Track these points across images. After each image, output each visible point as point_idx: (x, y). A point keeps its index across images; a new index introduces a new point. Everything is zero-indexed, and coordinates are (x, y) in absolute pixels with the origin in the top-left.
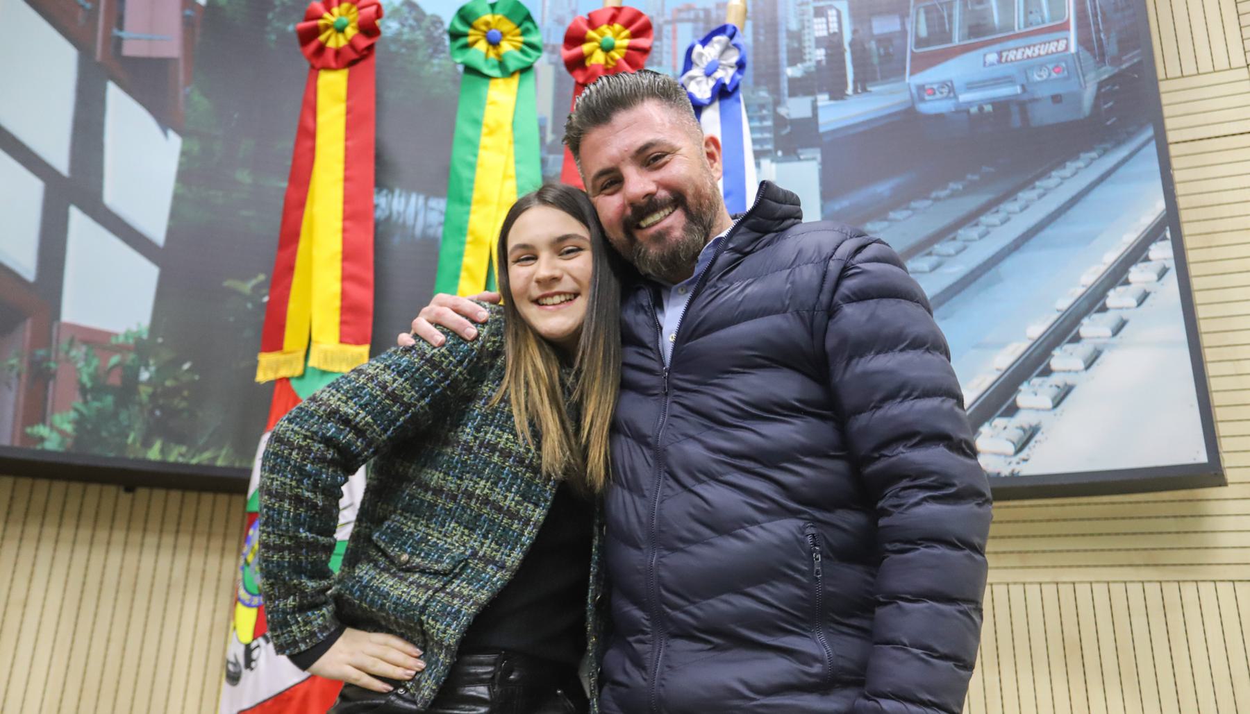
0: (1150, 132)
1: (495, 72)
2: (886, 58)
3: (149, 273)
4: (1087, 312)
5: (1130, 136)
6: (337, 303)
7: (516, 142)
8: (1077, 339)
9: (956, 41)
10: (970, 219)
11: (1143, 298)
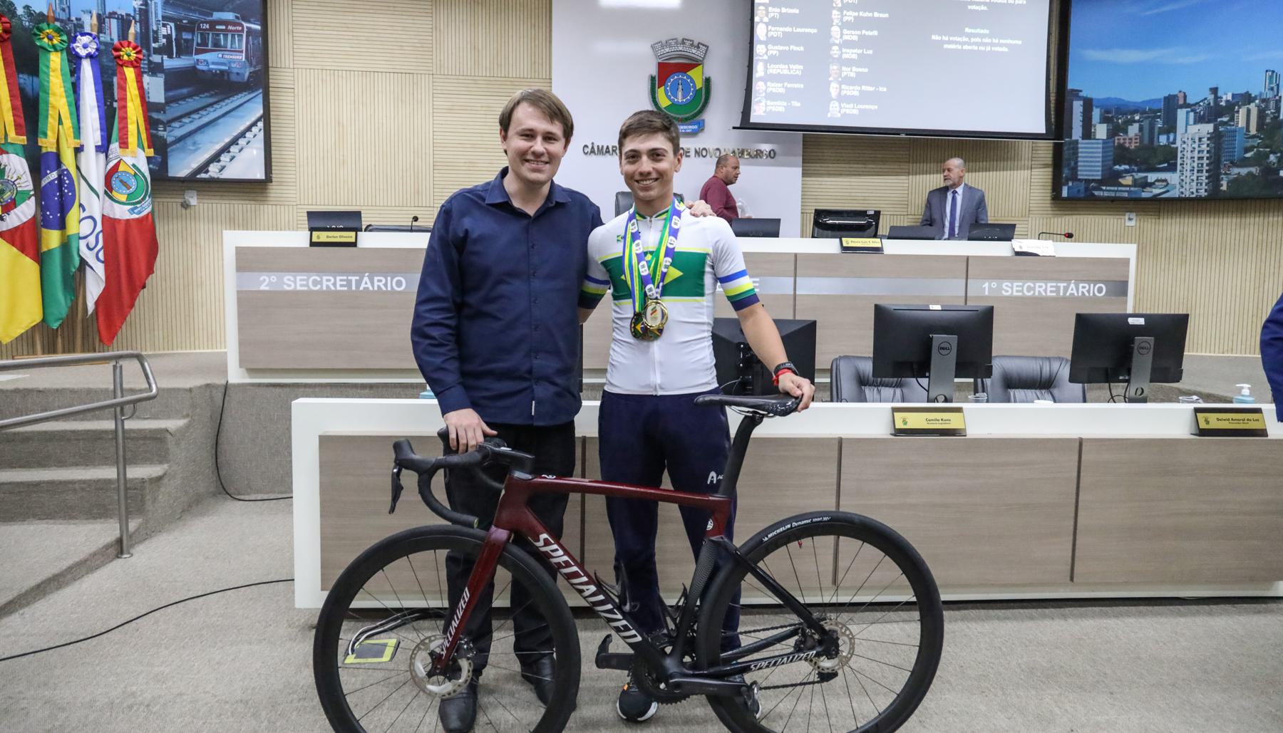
0: (261, 91)
2: (187, 47)
4: (240, 137)
5: (257, 90)
6: (13, 123)
7: (62, 75)
8: (237, 144)
10: (211, 105)
11: (255, 136)
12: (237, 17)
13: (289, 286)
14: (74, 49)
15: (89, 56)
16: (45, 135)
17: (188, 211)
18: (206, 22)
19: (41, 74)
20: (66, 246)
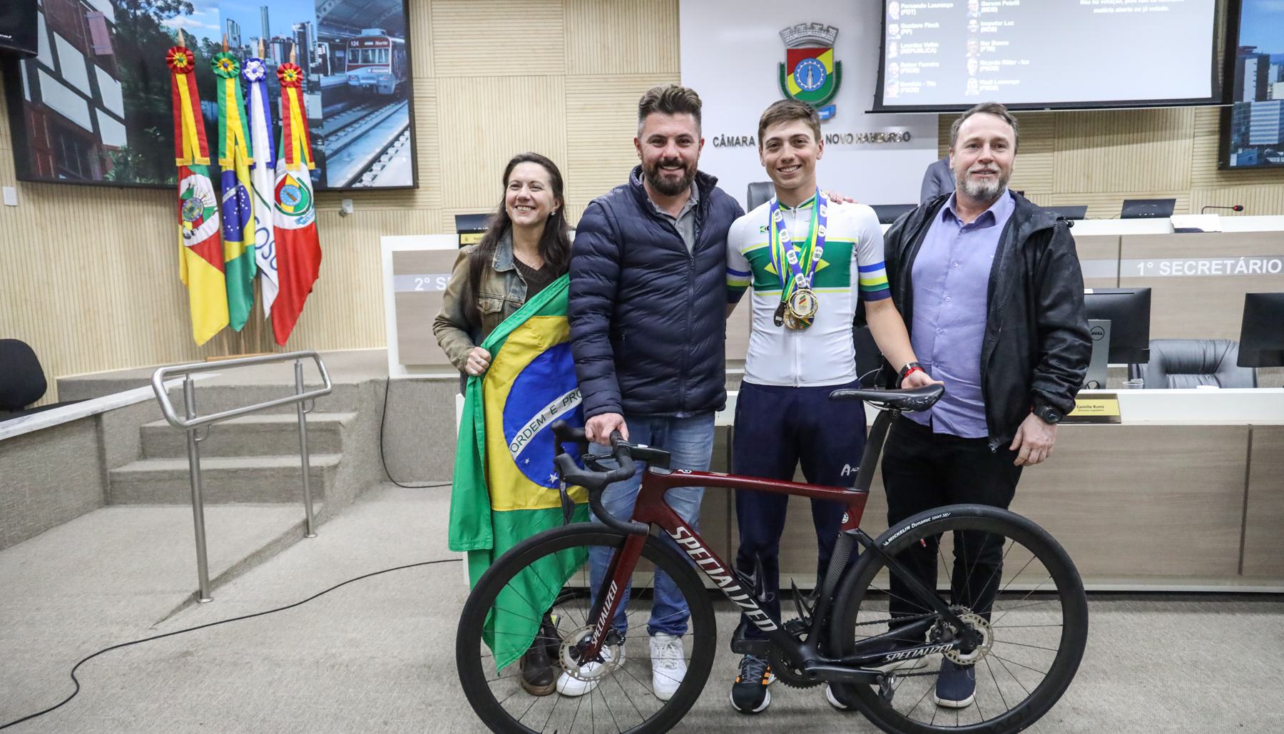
0: (406, 101)
1: (227, 77)
2: (340, 65)
3: (122, 128)
9: (360, 63)
10: (362, 118)
11: (402, 145)
12: (383, 33)
13: (1165, 271)
14: (245, 74)
15: (259, 80)
16: (224, 155)
17: (345, 218)
18: (356, 40)
19: (219, 101)
20: (244, 256)
